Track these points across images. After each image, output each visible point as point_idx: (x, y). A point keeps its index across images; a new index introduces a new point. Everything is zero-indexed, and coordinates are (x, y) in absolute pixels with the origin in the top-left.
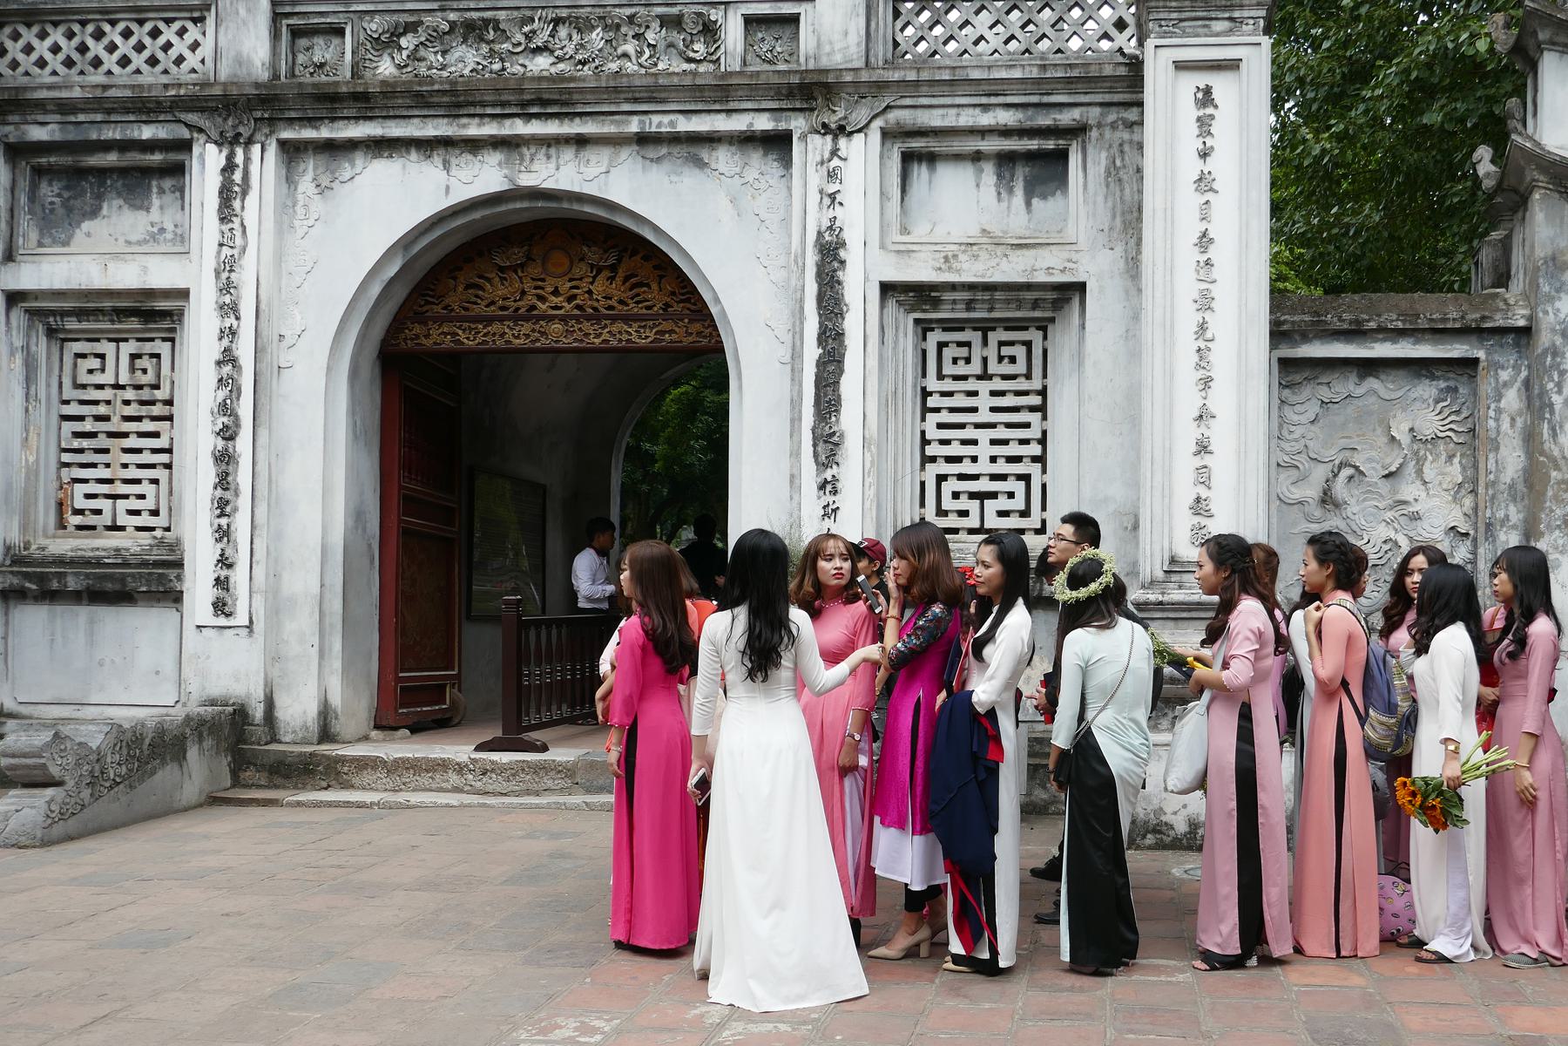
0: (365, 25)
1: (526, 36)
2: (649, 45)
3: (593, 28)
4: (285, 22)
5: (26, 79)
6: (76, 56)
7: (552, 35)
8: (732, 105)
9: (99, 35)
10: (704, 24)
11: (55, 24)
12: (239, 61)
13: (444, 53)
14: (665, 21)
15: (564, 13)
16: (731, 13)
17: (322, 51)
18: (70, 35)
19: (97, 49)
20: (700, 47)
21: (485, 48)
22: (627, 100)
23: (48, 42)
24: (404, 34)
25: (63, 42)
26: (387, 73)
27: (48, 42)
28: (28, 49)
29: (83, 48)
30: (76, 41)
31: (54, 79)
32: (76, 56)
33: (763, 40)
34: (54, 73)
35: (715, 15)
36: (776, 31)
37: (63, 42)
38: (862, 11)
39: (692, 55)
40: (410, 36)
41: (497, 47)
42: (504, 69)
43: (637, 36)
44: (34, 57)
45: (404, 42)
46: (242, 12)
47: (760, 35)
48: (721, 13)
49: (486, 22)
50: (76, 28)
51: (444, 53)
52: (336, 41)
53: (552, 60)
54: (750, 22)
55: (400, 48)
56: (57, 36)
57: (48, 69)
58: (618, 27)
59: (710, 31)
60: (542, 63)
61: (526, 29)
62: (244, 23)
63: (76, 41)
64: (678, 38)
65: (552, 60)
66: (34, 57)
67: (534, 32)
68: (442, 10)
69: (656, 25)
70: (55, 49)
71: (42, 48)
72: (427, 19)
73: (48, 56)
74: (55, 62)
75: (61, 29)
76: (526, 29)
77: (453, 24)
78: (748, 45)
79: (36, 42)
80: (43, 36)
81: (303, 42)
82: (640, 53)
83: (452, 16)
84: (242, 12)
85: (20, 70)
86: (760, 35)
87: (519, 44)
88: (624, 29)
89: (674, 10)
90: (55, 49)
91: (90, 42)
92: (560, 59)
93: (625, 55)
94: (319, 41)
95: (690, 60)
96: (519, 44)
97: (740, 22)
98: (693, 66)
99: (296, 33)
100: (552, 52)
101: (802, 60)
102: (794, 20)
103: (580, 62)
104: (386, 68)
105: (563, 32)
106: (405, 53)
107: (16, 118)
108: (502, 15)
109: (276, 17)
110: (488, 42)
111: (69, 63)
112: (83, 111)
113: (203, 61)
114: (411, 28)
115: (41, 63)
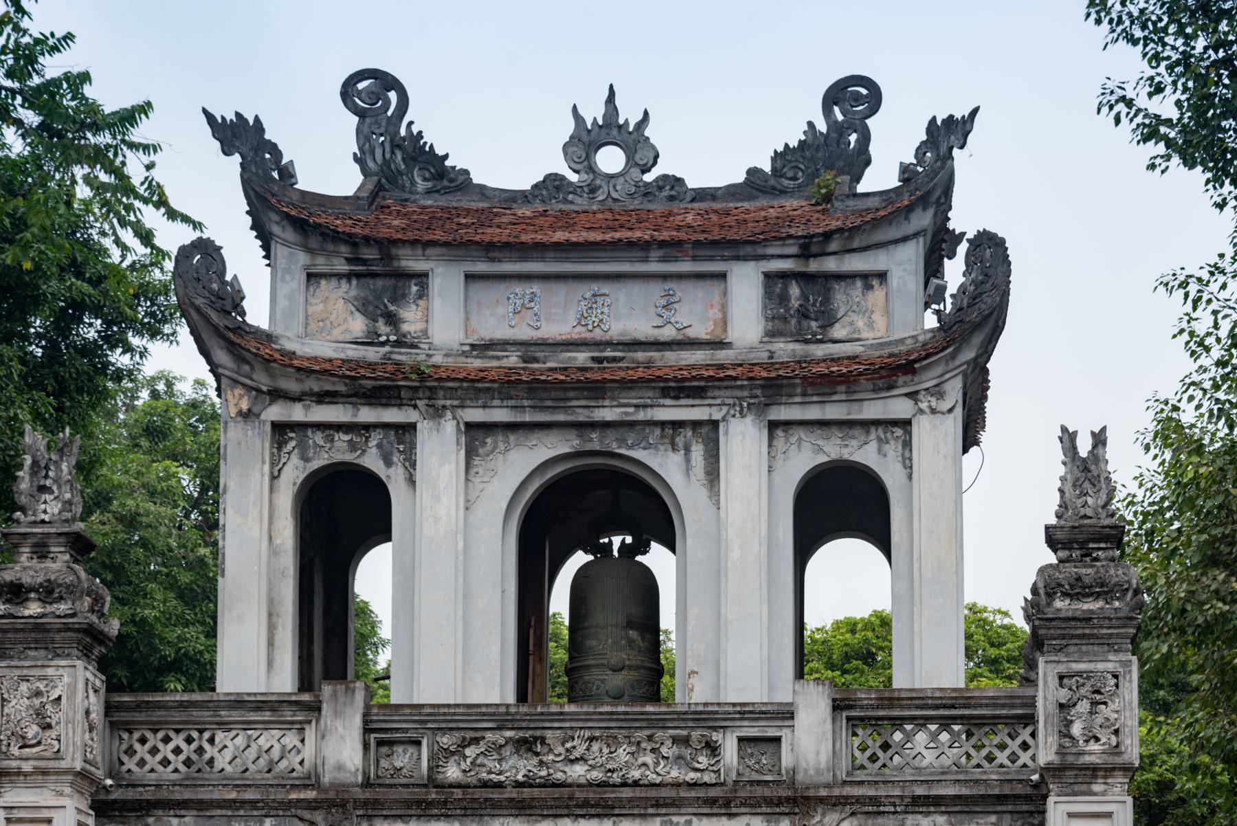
0: (438, 739)
1: (567, 750)
2: (663, 757)
3: (619, 744)
4: (373, 736)
5: (153, 775)
6: (194, 757)
7: (588, 749)
8: (734, 810)
9: (211, 741)
10: (707, 743)
11: (177, 731)
12: (340, 767)
13: (500, 761)
14: (676, 740)
15: (597, 733)
16: (728, 735)
17: (402, 758)
18: (189, 740)
19: (210, 751)
20: (703, 760)
21: (535, 761)
22: (652, 806)
23: (171, 746)
24: (469, 745)
25: (184, 746)
26: (455, 775)
27: (171, 746)
28: (154, 751)
29: (200, 751)
30: (194, 745)
31: (175, 776)
32: (194, 757)
33: (752, 755)
34: (176, 770)
35: (716, 736)
36: (763, 747)
37: (184, 746)
38: (830, 736)
39: (697, 766)
40: (473, 748)
41: (545, 759)
42: (549, 775)
43: (653, 750)
44: (159, 757)
45: (468, 752)
46: (340, 729)
47: (749, 751)
48: (721, 736)
49: (536, 739)
50: (195, 734)
51: (500, 761)
52: (411, 750)
53: (587, 768)
54: (741, 740)
55: (465, 757)
56: (178, 740)
57: (171, 768)
58: (639, 743)
59: (713, 749)
60: (578, 772)
61: (568, 745)
62: (342, 737)
63: (194, 745)
64: (687, 753)
65: (587, 768)
66: (159, 757)
67: (574, 747)
68: (499, 729)
69: (669, 743)
70: (177, 751)
71: (166, 750)
72: (489, 736)
73: (171, 757)
74: (177, 762)
75: (183, 735)
76: (568, 745)
77: (509, 740)
78: (741, 758)
79: (161, 746)
80: (167, 740)
81: (384, 750)
82: (657, 764)
83: (509, 734)
84: (340, 729)
85: (147, 767)
86: (749, 751)
87: (560, 755)
88: (643, 745)
89: (685, 733)
90: (177, 751)
91: (206, 746)
92: (593, 767)
93: (644, 764)
94: (399, 749)
95: (696, 770)
96: (560, 755)
97: (735, 741)
98: (699, 775)
99: (380, 743)
100: (586, 761)
101: (783, 771)
102: (778, 740)
103: (610, 770)
104: (452, 772)
105: (596, 746)
106: (469, 761)
107: (160, 813)
108: (549, 734)
109: (367, 730)
110: (537, 754)
111: (188, 763)
112: (221, 807)
113: (301, 763)
114: (476, 741)
115: (165, 762)
